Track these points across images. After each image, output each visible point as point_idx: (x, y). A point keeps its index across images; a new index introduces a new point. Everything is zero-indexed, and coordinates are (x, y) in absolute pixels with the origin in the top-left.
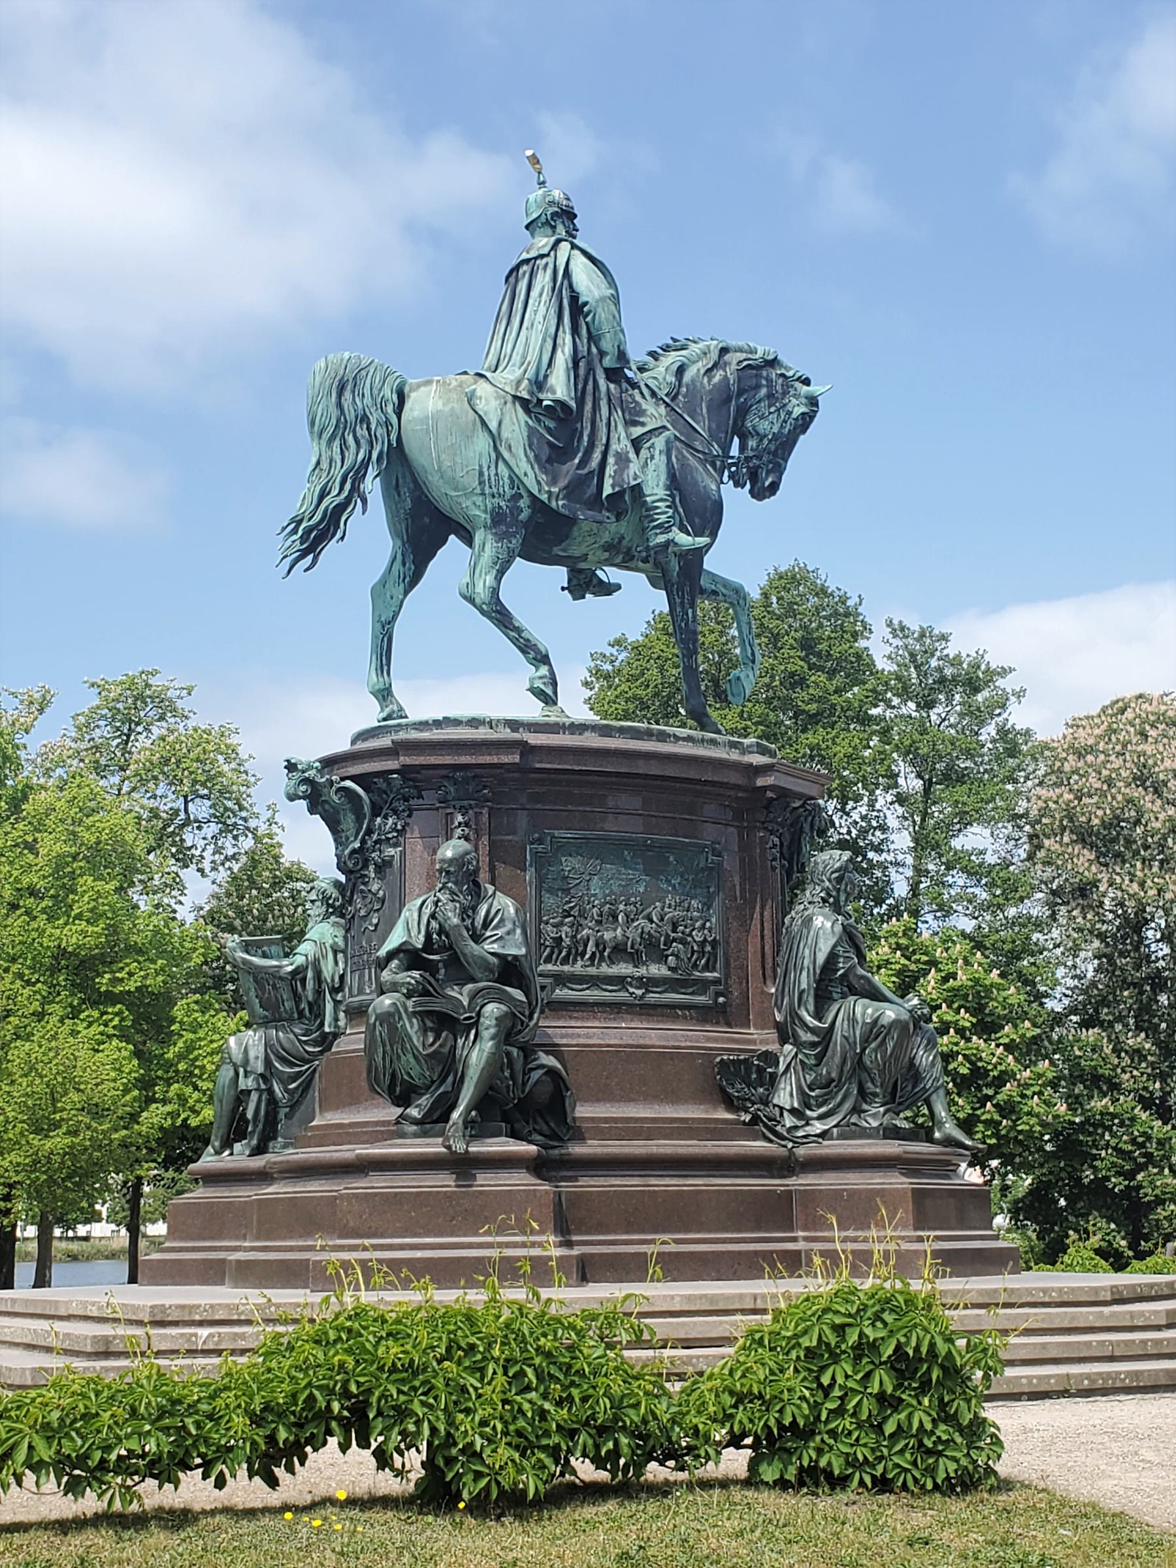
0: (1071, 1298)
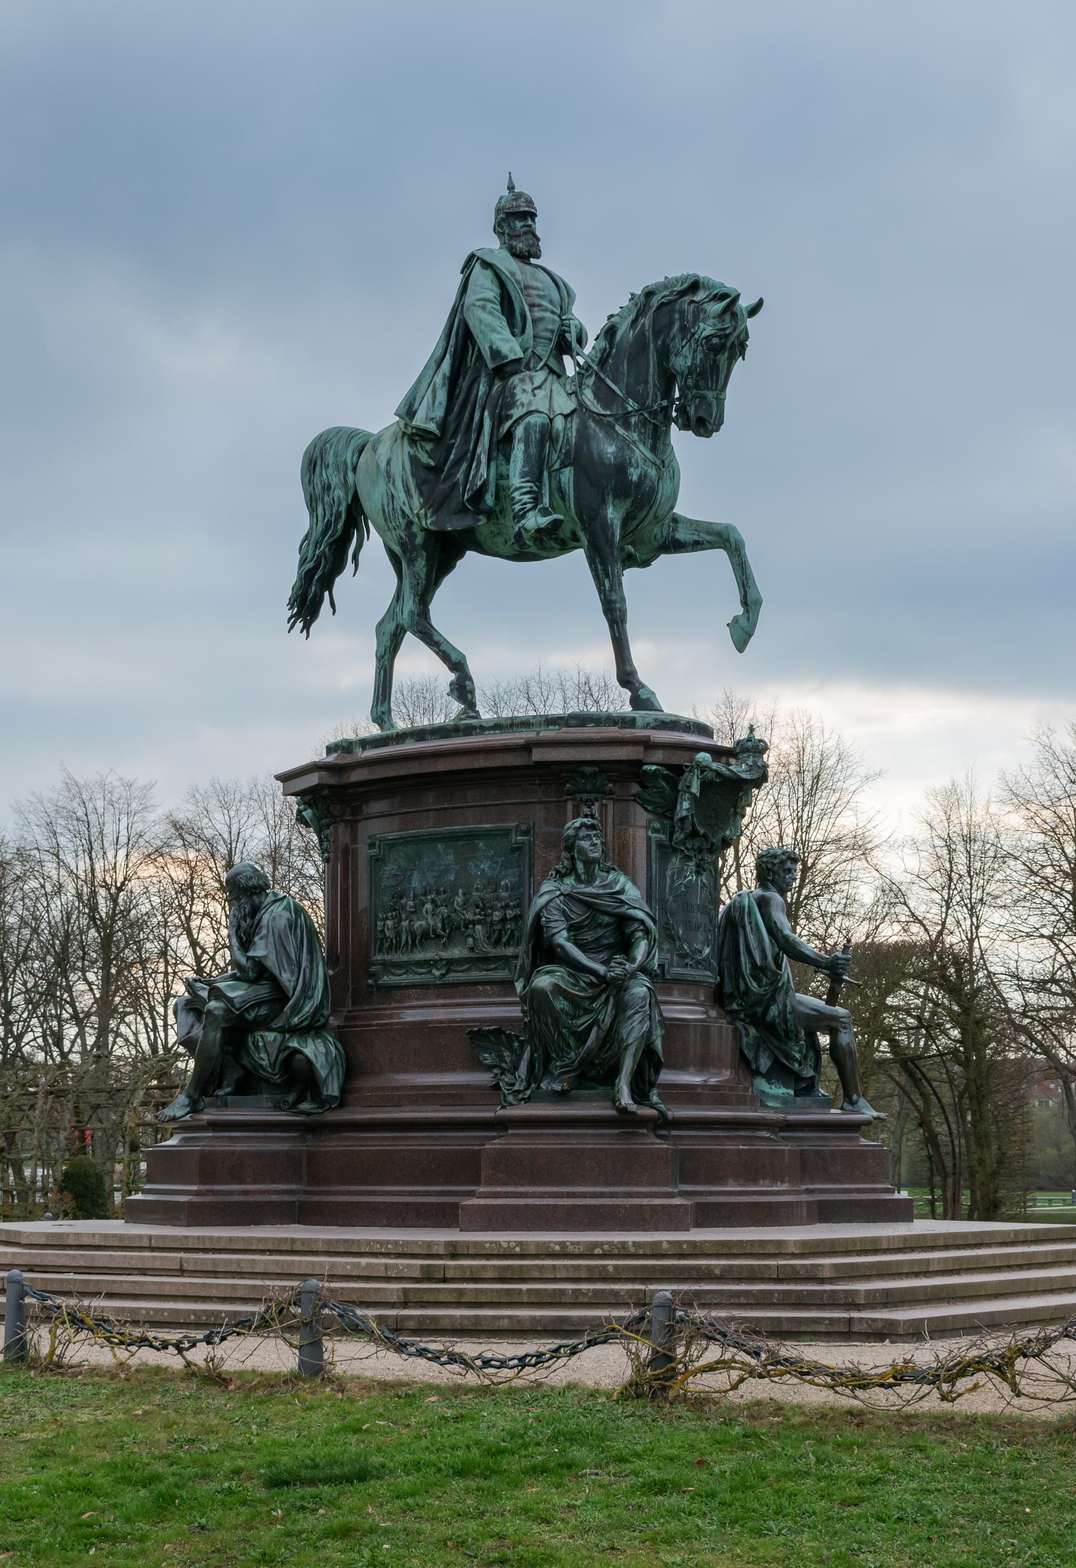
0: (406, 1250)
